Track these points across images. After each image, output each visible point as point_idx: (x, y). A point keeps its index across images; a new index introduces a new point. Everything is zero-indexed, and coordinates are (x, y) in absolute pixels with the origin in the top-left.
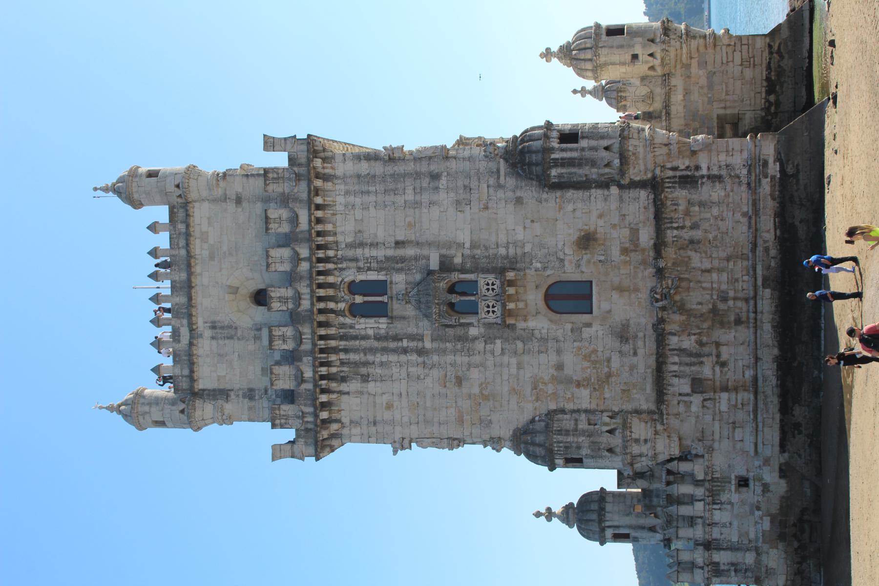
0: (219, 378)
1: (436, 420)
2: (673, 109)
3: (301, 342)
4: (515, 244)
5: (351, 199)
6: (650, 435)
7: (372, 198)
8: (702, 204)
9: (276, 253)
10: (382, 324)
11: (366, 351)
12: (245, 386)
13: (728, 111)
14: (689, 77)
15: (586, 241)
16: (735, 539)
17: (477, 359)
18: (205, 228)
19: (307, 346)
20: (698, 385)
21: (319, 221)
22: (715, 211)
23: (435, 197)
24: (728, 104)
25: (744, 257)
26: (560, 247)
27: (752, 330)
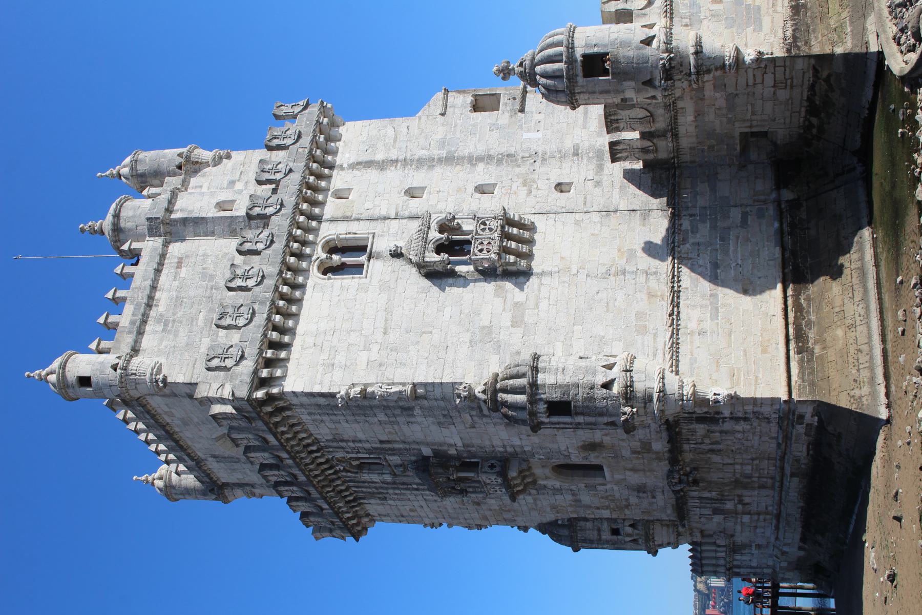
2: (682, 130)
3: (310, 494)
4: (513, 446)
5: (318, 417)
6: (672, 540)
8: (721, 432)
11: (376, 488)
13: (755, 130)
14: (702, 99)
15: (592, 447)
16: (754, 564)
18: (166, 409)
22: (739, 436)
23: (413, 420)
24: (754, 123)
25: (769, 459)
26: (563, 448)
27: (776, 495)
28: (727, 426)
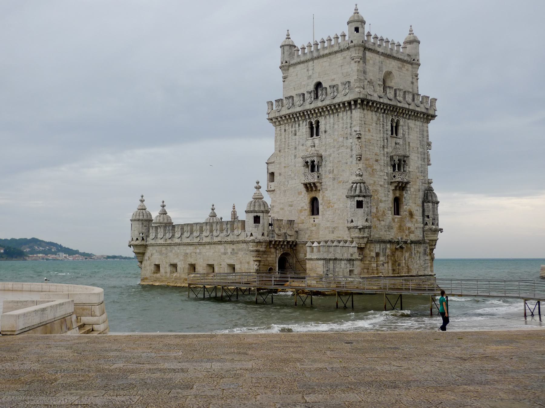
0: (369, 60)
1: (367, 149)
3: (390, 100)
7: (419, 136)
9: (411, 96)
10: (390, 133)
12: (368, 70)
15: (411, 214)
16: (337, 270)
17: (383, 169)
18: (406, 67)
19: (389, 102)
20: (378, 255)
21: (417, 114)
22: (418, 262)
27: (392, 275)
28: (422, 258)
